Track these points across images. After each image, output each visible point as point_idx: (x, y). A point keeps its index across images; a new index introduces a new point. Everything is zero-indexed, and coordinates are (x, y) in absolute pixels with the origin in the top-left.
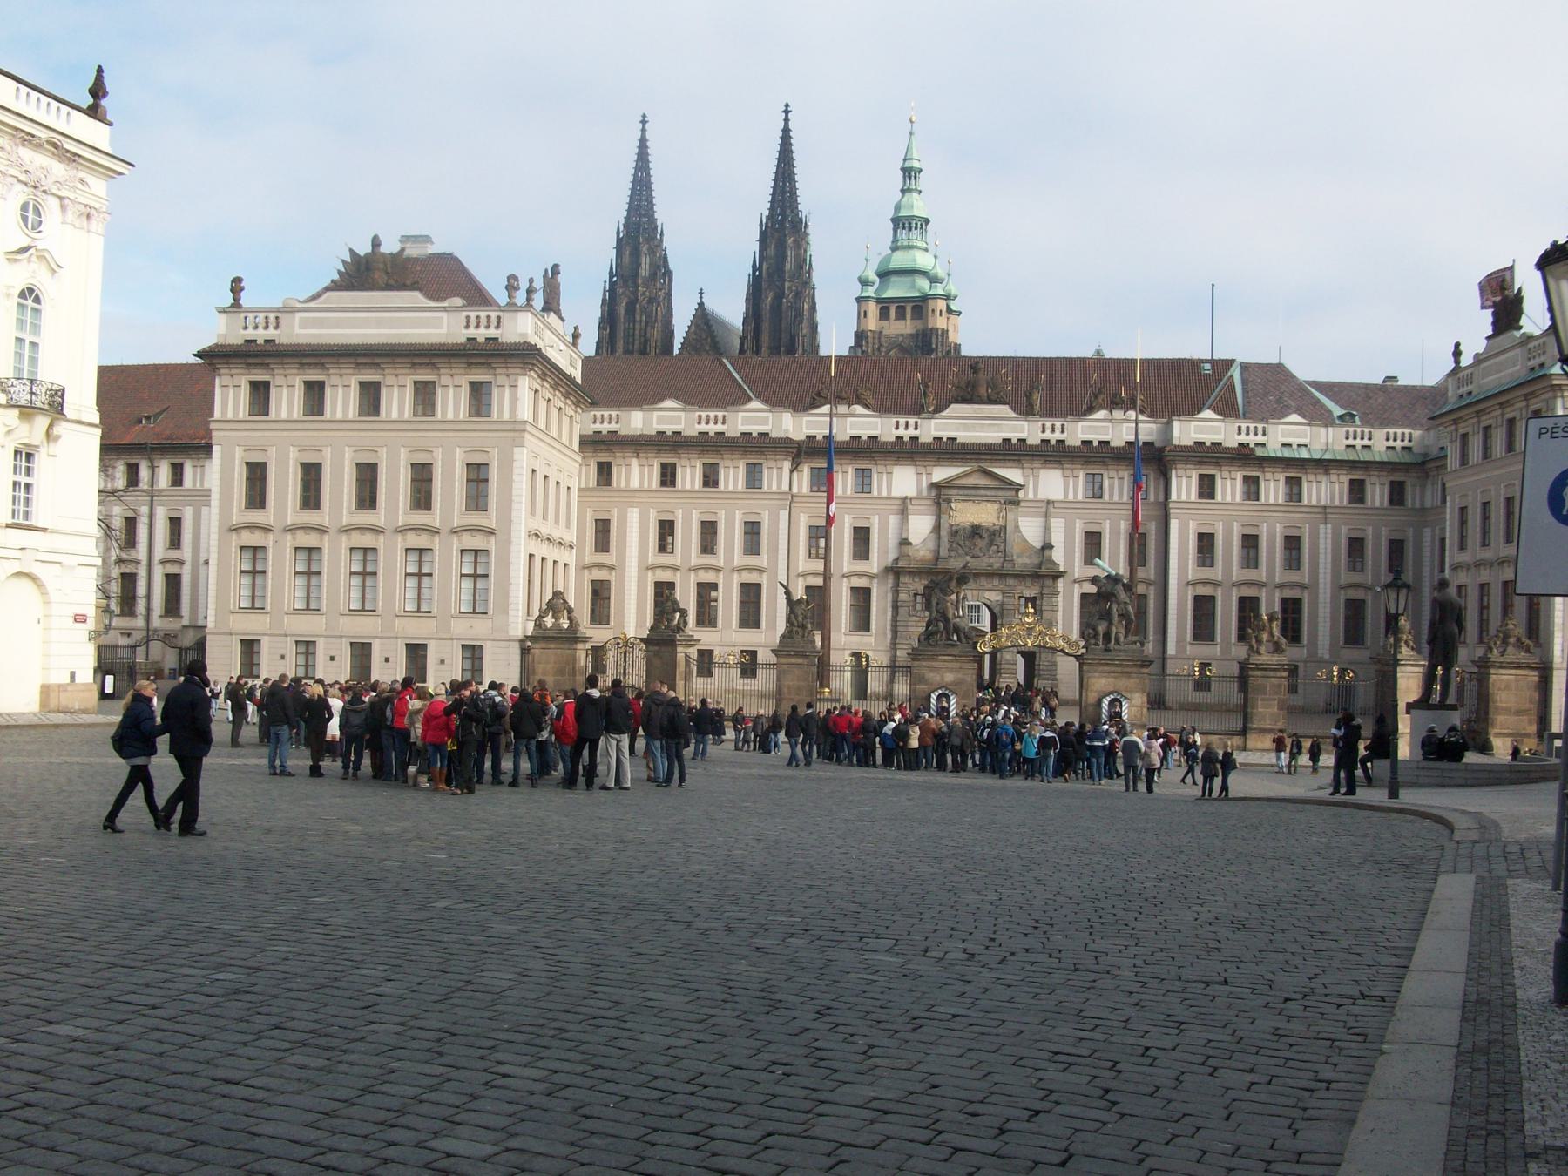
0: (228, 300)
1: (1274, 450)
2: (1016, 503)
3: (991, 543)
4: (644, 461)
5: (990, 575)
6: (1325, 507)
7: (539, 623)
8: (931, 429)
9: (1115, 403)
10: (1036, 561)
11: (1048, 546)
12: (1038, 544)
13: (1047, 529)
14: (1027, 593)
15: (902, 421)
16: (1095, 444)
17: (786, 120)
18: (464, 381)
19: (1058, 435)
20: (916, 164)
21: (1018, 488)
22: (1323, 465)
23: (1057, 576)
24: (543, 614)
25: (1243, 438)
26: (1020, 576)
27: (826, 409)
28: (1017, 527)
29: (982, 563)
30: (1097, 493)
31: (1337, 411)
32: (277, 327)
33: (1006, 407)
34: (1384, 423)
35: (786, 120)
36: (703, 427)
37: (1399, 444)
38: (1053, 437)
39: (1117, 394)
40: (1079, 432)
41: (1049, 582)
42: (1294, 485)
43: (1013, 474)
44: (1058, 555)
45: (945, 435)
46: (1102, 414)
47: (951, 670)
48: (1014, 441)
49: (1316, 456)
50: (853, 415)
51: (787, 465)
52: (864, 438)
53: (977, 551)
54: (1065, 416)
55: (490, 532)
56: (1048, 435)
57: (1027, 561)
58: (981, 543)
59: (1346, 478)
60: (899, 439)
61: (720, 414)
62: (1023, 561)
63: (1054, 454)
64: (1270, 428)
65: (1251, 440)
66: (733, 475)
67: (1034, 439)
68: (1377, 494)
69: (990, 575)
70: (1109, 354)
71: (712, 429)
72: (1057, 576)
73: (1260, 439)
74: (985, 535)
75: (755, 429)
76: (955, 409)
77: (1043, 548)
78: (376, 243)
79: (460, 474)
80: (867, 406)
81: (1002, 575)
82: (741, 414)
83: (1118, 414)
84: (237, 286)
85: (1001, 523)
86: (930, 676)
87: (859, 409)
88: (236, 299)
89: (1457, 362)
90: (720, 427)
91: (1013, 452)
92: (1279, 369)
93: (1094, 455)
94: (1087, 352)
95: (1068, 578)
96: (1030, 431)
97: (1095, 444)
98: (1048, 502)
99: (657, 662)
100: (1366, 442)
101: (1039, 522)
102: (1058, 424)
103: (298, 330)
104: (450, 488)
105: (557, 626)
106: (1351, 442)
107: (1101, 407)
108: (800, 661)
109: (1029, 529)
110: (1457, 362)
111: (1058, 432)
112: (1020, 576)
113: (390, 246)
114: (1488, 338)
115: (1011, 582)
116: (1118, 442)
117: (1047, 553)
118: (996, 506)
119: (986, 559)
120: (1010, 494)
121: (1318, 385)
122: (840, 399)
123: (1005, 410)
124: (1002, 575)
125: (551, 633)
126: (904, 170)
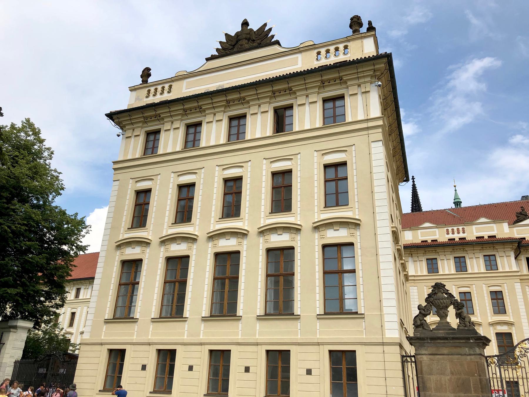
0: (139, 81)
7: (419, 323)
18: (317, 98)
20: (459, 200)
24: (423, 312)
32: (169, 92)
36: (451, 236)
55: (353, 224)
61: (461, 228)
66: (476, 264)
71: (457, 237)
75: (486, 234)
78: (245, 24)
79: (318, 176)
84: (146, 74)
88: (145, 81)
90: (462, 235)
103: (184, 91)
104: (309, 187)
105: (444, 325)
113: (254, 26)
125: (441, 333)
126: (454, 203)
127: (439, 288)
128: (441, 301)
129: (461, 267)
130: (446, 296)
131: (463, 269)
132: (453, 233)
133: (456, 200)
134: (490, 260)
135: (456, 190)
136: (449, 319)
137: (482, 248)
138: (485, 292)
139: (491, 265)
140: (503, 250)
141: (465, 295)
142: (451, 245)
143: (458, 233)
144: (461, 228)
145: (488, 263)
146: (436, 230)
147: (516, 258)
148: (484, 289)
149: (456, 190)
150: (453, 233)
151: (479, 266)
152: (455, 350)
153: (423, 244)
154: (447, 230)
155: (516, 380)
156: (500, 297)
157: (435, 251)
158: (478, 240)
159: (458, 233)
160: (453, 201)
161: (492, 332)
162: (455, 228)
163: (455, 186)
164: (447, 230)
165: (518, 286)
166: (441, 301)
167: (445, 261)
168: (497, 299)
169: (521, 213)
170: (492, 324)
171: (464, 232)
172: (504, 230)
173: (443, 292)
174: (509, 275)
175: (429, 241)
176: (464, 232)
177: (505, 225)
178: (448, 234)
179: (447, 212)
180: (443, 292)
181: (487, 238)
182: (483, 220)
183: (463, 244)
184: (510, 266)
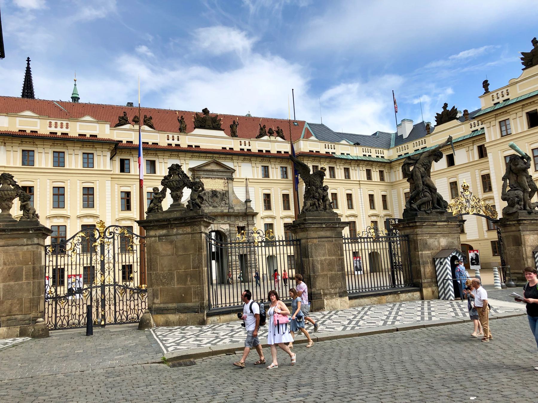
1: (338, 154)
2: (232, 179)
3: (222, 199)
4: (9, 148)
5: (223, 215)
6: (359, 181)
8: (185, 141)
9: (271, 133)
10: (244, 208)
11: (248, 201)
12: (243, 200)
13: (247, 192)
14: (241, 224)
15: (171, 136)
16: (264, 152)
17: (28, 64)
19: (247, 147)
21: (233, 171)
22: (358, 162)
23: (254, 215)
25: (327, 150)
26: (237, 216)
27: (127, 126)
28: (233, 191)
29: (219, 210)
30: (266, 174)
31: (352, 143)
33: (222, 132)
34: (375, 148)
35: (28, 64)
36: (53, 130)
37: (380, 155)
38: (246, 148)
39: (270, 129)
40: (256, 146)
41: (250, 219)
42: (347, 170)
43: (229, 164)
44: (253, 205)
45: (194, 144)
46: (266, 138)
47: (444, 235)
48: (228, 149)
49: (356, 158)
50: (144, 131)
51: (109, 155)
52: (150, 143)
53: (215, 204)
54: (249, 137)
56: (243, 147)
57: (239, 208)
58: (217, 200)
59: (365, 169)
60: (170, 145)
61: (65, 123)
62: (238, 208)
63: (247, 156)
64: (336, 146)
65: (331, 151)
66: (74, 159)
67: (237, 148)
68: (375, 176)
69: (223, 215)
70: (253, 115)
71: (59, 131)
72: (254, 215)
73: (333, 151)
74: (219, 196)
75: (88, 133)
76: (198, 131)
77: (246, 202)
80: (151, 127)
81: (228, 215)
82: (78, 124)
83: (272, 138)
85: (226, 189)
86: (431, 241)
87: (146, 128)
89: (487, 91)
90: (64, 130)
91: (229, 154)
92: (322, 125)
93: (263, 156)
94: (245, 115)
95: (259, 216)
96: (235, 144)
97: (264, 152)
98: (246, 179)
99: (164, 248)
100: (370, 154)
101: (244, 189)
102: (247, 142)
106: (365, 153)
107: (265, 134)
108: (328, 234)
109: (239, 193)
110: (487, 91)
111: (247, 145)
112: (237, 216)
114: (523, 69)
115: (233, 219)
116: (274, 151)
117: (248, 204)
118: (223, 181)
119: (220, 208)
120: (228, 174)
121: (338, 133)
122: (136, 121)
123: (221, 133)
124: (228, 215)
126: (72, 98)
127: (6, 179)
128: (6, 192)
129: (59, 162)
130: (13, 188)
131: (61, 164)
132: (56, 127)
133: (74, 96)
134: (88, 158)
135: (75, 85)
136: (11, 212)
137: (83, 145)
138: (78, 187)
139: (88, 163)
140: (101, 149)
141: (59, 190)
142: (52, 139)
143: (62, 127)
144: (65, 123)
145: (86, 161)
146: (38, 120)
147: (111, 159)
148: (78, 184)
149: (75, 85)
150: (56, 127)
151: (76, 163)
152: (11, 242)
153: (21, 133)
154: (50, 123)
155: (62, 267)
156: (91, 193)
157: (34, 142)
158: (80, 137)
159: (62, 127)
160: (71, 96)
161: (78, 224)
162: (59, 123)
163: (75, 81)
164: (50, 123)
165: (108, 184)
166: (6, 192)
167: (43, 155)
168: (88, 195)
169: (123, 118)
170: (80, 217)
171: (67, 128)
172: (105, 131)
173: (9, 183)
174: (103, 173)
175: (28, 131)
176: (67, 128)
177: (107, 126)
178: (50, 126)
179: (54, 104)
180: (9, 183)
181: (89, 136)
182: (88, 118)
183: (65, 139)
184: (105, 165)
